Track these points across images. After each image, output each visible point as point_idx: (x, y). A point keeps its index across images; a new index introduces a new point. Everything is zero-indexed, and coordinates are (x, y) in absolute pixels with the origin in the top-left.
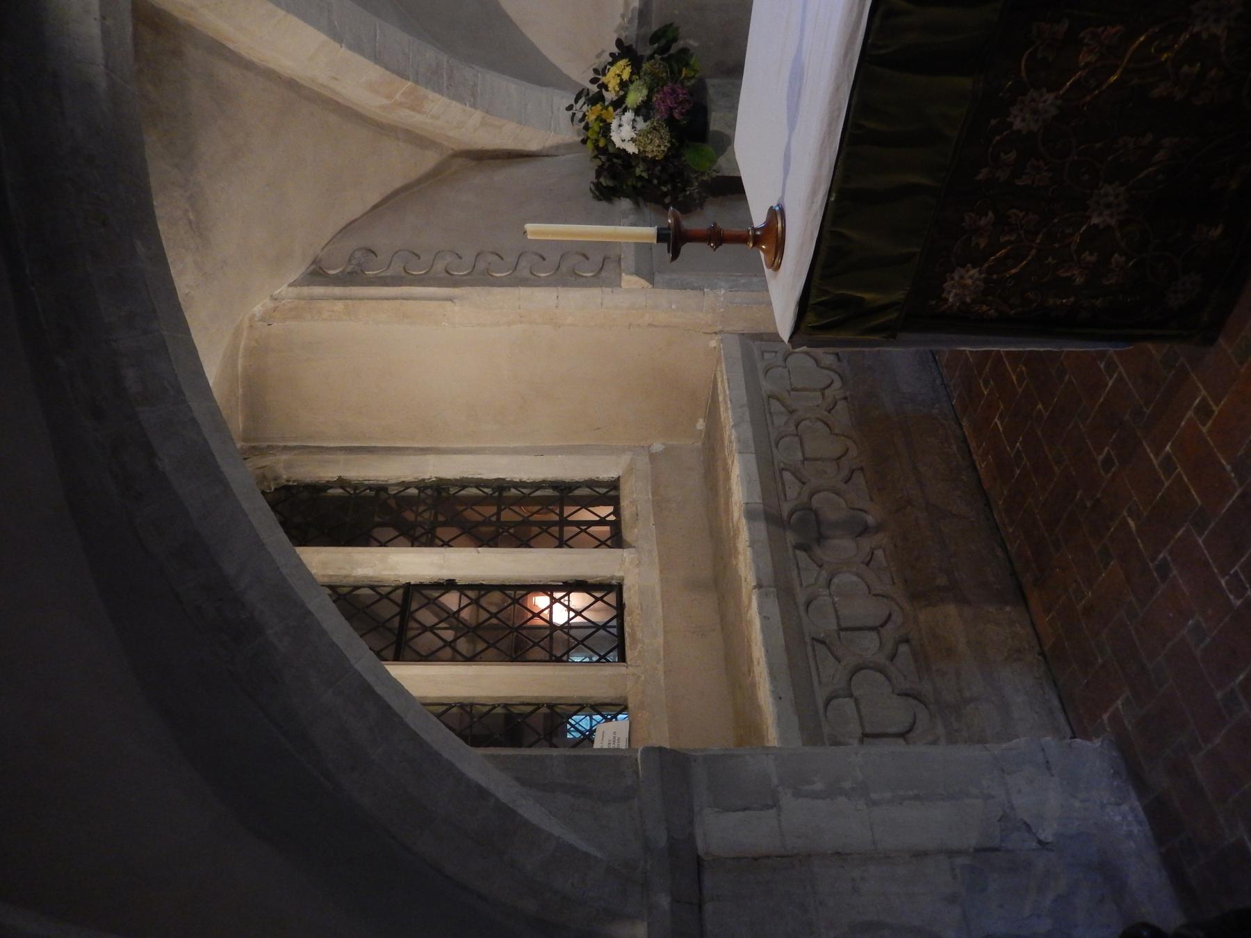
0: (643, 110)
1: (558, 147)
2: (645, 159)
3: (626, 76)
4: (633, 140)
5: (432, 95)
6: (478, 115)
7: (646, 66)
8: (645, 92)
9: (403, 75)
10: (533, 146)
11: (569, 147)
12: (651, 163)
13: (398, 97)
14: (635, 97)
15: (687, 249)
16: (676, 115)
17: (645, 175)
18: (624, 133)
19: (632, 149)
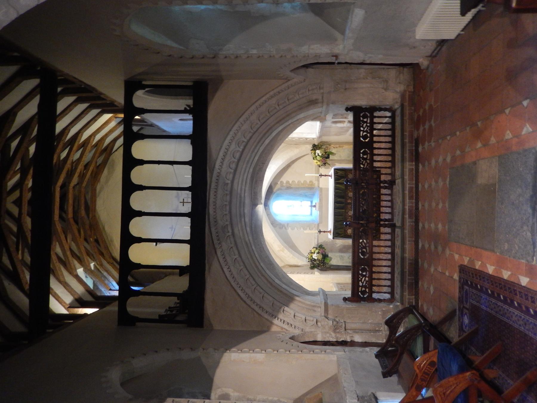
0: (318, 253)
1: (304, 265)
2: (319, 260)
3: (315, 250)
4: (316, 256)
5: (286, 250)
6: (292, 255)
7: (318, 248)
8: (318, 251)
9: (282, 245)
10: (300, 264)
11: (306, 265)
12: (319, 260)
13: (281, 248)
14: (317, 251)
15: (321, 233)
16: (323, 253)
17: (319, 263)
18: (315, 256)
19: (316, 258)
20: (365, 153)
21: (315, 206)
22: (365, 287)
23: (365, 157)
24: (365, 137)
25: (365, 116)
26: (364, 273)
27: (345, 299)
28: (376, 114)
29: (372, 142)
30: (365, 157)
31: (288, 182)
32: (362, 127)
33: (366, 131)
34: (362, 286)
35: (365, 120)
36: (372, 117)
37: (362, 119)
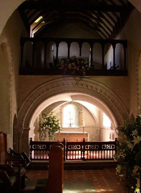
20: (97, 147)
21: (70, 126)
22: (37, 147)
23: (95, 147)
24: (104, 147)
25: (113, 147)
26: (43, 147)
27: (31, 138)
28: (114, 151)
29: (102, 150)
30: (95, 147)
31: (82, 112)
32: (109, 146)
33: (106, 147)
34: (37, 146)
35: (111, 147)
36: (113, 150)
37: (112, 145)
